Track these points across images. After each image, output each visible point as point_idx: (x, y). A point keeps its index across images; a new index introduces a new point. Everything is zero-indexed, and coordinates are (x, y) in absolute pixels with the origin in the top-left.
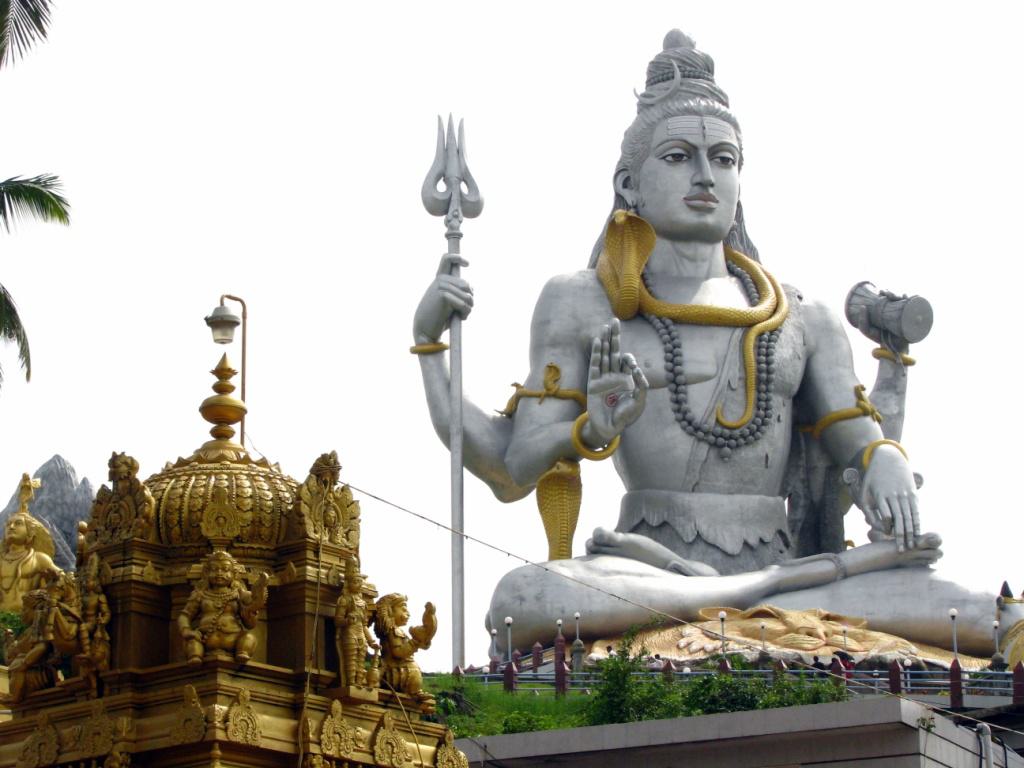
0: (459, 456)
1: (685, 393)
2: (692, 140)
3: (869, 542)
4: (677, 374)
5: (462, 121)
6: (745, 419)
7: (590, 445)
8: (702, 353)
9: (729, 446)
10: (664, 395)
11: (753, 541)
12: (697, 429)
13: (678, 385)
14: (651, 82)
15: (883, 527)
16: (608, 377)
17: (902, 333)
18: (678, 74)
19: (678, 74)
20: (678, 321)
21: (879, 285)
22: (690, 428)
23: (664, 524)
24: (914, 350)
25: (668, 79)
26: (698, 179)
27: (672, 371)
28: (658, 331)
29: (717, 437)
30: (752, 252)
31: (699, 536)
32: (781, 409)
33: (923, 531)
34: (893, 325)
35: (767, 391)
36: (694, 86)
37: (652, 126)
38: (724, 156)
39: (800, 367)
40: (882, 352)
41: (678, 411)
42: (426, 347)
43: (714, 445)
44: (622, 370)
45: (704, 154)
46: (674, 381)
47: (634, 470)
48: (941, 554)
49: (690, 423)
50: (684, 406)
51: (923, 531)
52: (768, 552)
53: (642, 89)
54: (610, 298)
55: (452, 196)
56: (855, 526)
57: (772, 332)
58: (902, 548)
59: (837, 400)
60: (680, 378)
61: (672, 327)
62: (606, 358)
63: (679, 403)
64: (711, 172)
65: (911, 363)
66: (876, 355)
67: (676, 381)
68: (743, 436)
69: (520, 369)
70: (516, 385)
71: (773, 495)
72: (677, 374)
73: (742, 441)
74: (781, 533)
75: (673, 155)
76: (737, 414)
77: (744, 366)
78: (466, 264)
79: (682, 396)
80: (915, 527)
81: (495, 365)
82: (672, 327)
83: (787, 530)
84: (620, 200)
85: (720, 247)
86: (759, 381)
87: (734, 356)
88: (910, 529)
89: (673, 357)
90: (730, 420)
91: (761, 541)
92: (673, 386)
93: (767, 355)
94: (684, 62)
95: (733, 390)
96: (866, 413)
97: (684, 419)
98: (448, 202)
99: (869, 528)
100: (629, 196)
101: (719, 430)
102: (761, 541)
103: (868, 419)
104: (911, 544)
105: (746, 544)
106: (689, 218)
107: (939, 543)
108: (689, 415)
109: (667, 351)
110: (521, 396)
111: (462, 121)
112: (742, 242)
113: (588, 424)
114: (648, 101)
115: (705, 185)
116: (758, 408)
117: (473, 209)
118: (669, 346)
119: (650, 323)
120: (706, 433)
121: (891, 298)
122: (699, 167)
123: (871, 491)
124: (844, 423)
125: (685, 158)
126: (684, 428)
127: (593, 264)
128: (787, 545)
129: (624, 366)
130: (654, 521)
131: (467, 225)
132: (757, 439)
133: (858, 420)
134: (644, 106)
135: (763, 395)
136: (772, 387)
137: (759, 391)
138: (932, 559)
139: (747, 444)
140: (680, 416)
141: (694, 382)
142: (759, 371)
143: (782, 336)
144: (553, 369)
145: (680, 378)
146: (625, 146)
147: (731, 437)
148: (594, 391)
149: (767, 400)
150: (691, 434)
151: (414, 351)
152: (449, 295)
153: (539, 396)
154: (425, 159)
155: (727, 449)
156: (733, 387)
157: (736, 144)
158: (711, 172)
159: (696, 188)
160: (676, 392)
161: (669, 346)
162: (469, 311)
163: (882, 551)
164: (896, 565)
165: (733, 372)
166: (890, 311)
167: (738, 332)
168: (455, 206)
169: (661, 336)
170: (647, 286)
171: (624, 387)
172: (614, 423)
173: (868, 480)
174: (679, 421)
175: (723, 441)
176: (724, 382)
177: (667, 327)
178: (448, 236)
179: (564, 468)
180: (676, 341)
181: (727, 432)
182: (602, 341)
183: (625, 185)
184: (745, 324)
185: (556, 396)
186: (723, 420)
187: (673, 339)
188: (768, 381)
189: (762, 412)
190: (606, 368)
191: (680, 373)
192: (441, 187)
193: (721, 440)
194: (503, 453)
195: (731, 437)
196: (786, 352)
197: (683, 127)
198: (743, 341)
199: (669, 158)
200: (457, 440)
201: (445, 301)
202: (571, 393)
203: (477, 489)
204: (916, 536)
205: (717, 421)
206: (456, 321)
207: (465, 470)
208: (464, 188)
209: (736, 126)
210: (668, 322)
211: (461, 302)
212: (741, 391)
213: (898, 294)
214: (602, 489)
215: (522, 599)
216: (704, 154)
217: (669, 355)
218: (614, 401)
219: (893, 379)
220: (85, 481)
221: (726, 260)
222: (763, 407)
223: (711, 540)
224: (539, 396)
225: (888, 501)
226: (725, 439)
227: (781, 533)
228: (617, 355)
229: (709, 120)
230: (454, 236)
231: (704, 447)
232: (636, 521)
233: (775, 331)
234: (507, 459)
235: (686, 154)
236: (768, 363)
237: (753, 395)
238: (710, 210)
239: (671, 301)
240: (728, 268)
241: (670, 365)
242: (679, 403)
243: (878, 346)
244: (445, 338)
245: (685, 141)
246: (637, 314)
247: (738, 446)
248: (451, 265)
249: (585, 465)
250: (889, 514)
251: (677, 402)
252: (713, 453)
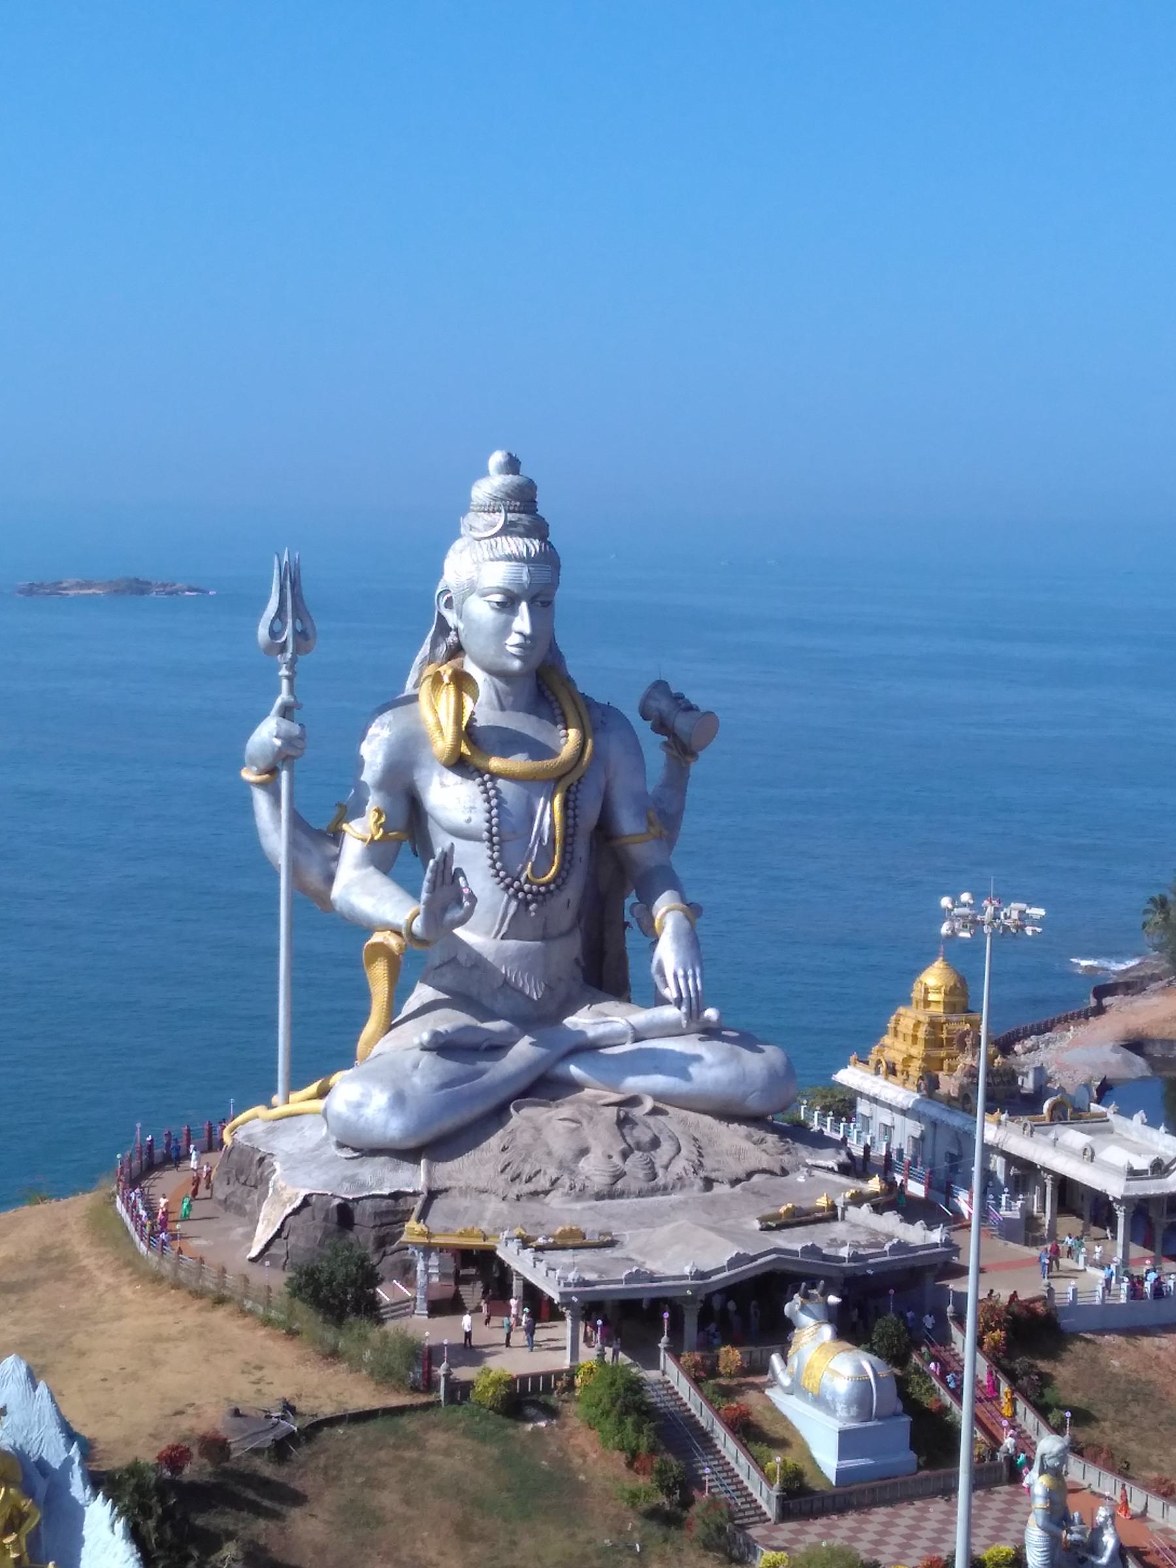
25: (494, 512)
29: (526, 893)
32: (582, 849)
59: (628, 822)
88: (694, 1007)
101: (526, 887)
135: (569, 849)
166: (682, 723)
190: (439, 880)
215: (361, 1116)
218: (445, 910)
219: (677, 777)
225: (676, 976)
243: (665, 738)
250: (675, 995)
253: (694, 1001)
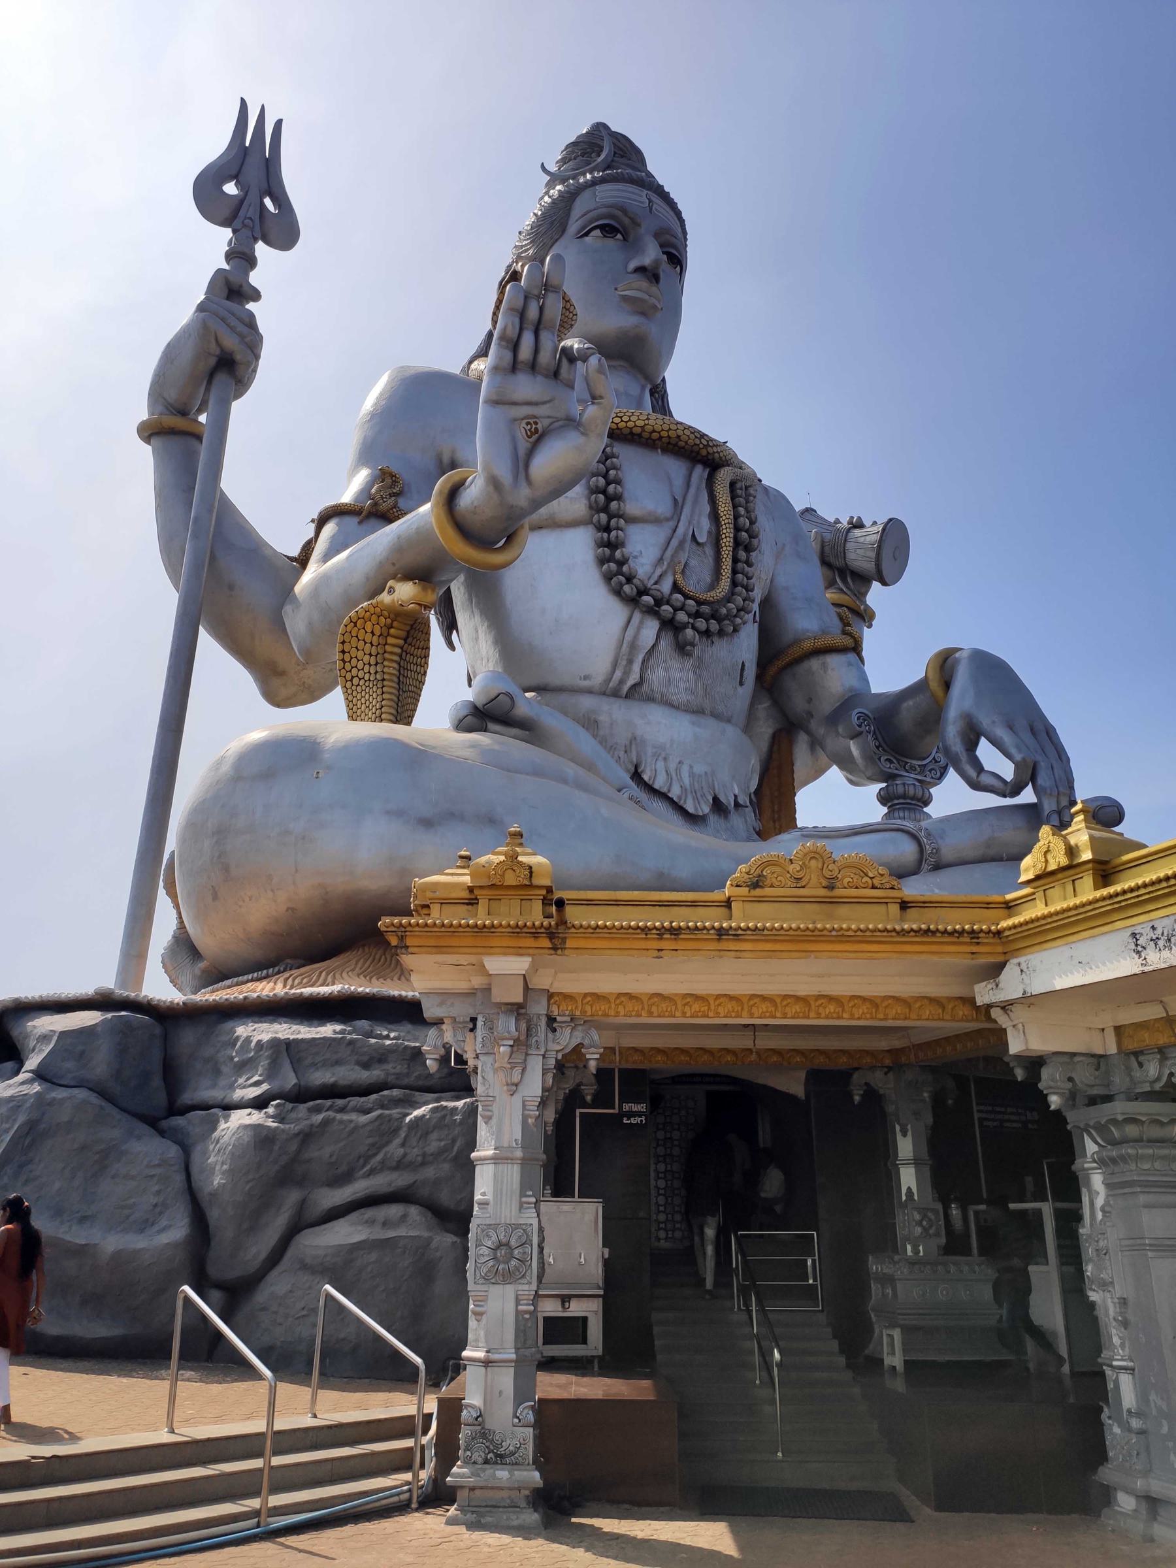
5: (279, 124)
9: (694, 628)
12: (643, 592)
13: (611, 517)
29: (676, 610)
43: (669, 625)
86: (737, 543)
91: (737, 805)
92: (603, 517)
95: (698, 544)
111: (279, 124)
116: (734, 584)
120: (659, 602)
125: (619, 236)
139: (721, 633)
142: (737, 529)
155: (689, 632)
156: (700, 541)
188: (748, 549)
199: (597, 232)
205: (676, 588)
212: (709, 551)
226: (689, 615)
248: (232, 290)
252: (666, 640)
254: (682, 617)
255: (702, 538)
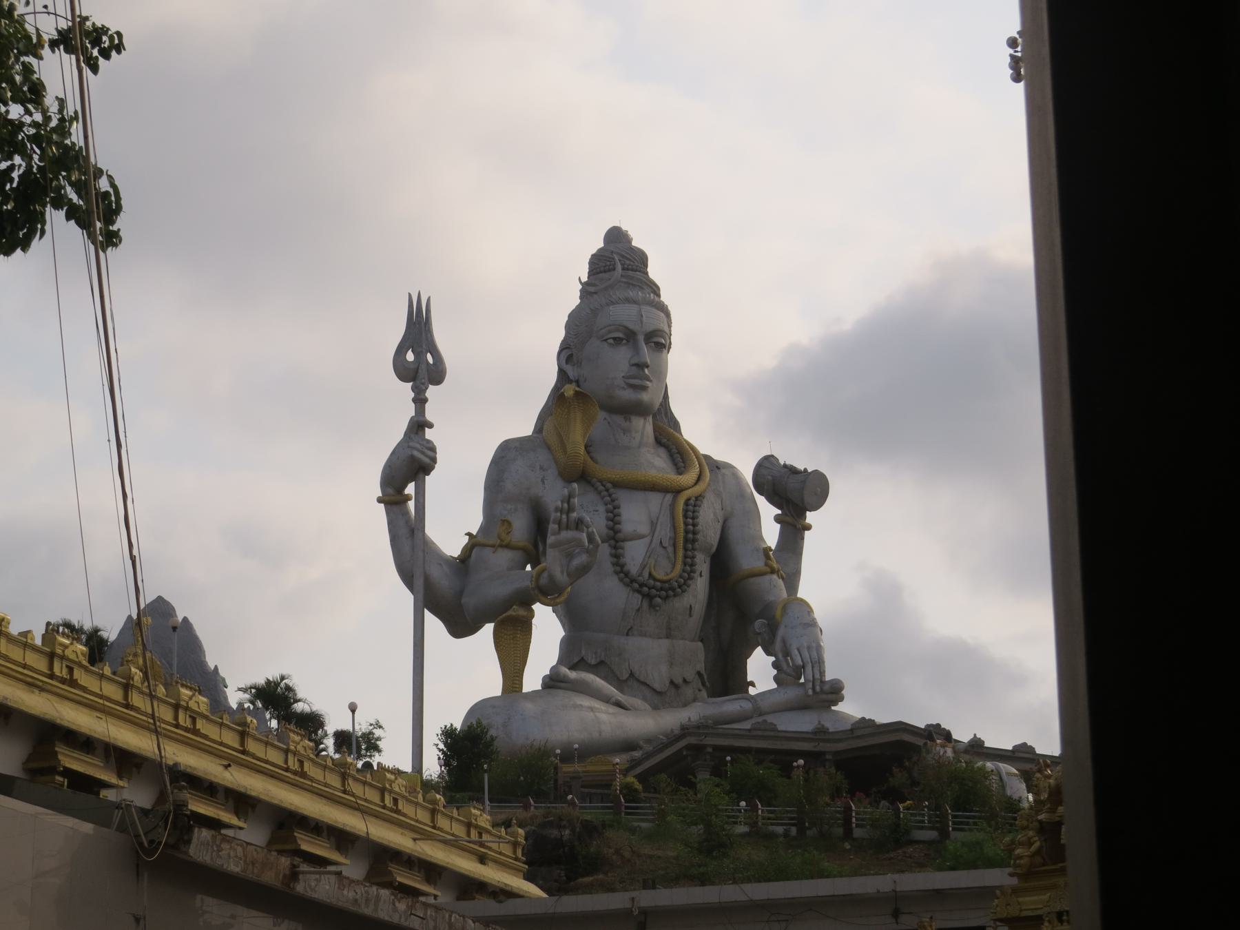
0: (421, 595)
1: (622, 548)
2: (631, 327)
3: (775, 686)
4: (616, 532)
6: (673, 575)
7: (547, 593)
8: (636, 514)
10: (605, 550)
11: (679, 681)
12: (633, 581)
14: (592, 273)
15: (785, 673)
16: (566, 535)
17: (802, 499)
18: (619, 267)
19: (619, 267)
20: (618, 485)
21: (783, 459)
22: (627, 580)
23: (602, 663)
24: (811, 517)
25: (609, 270)
26: (635, 361)
27: (612, 529)
28: (600, 493)
30: (675, 425)
31: (632, 675)
32: (703, 565)
33: (829, 677)
34: (796, 493)
35: (694, 549)
36: (632, 278)
37: (595, 312)
38: (659, 341)
39: (719, 527)
40: (788, 519)
41: (614, 564)
42: (393, 498)
44: (577, 528)
45: (641, 338)
46: (613, 538)
47: (572, 618)
48: (842, 699)
49: (627, 575)
50: (622, 560)
51: (829, 677)
52: (688, 692)
53: (585, 279)
54: (556, 462)
55: (419, 361)
56: (760, 670)
57: (697, 498)
58: (810, 692)
59: (747, 561)
60: (620, 535)
61: (612, 490)
62: (564, 516)
63: (617, 557)
64: (646, 354)
65: (809, 528)
66: (778, 519)
67: (615, 538)
68: (673, 590)
69: (474, 520)
70: (469, 534)
71: (693, 640)
72: (616, 532)
73: (671, 593)
74: (699, 673)
75: (614, 339)
76: (664, 571)
77: (674, 527)
78: (431, 426)
79: (620, 551)
80: (822, 673)
81: (454, 514)
82: (612, 490)
83: (703, 672)
84: (563, 376)
85: (650, 419)
86: (686, 540)
87: (665, 520)
88: (817, 676)
89: (614, 518)
90: (660, 575)
91: (685, 681)
92: (612, 542)
93: (693, 518)
94: (623, 256)
96: (773, 571)
97: (622, 571)
98: (417, 371)
99: (775, 672)
100: (570, 370)
102: (685, 681)
103: (775, 576)
104: (818, 688)
105: (672, 682)
106: (627, 395)
107: (841, 689)
108: (626, 568)
109: (607, 511)
110: (474, 544)
112: (666, 414)
113: (545, 575)
114: (592, 289)
115: (641, 366)
116: (685, 564)
117: (437, 375)
118: (610, 507)
119: (589, 482)
120: (642, 585)
121: (792, 470)
122: (637, 350)
123: (784, 641)
124: (752, 580)
126: (621, 580)
127: (539, 428)
128: (703, 684)
129: (579, 524)
130: (593, 662)
131: (432, 392)
132: (683, 591)
133: (767, 577)
134: (587, 291)
136: (697, 545)
137: (686, 549)
138: (835, 704)
140: (618, 569)
141: (631, 540)
142: (686, 532)
143: (705, 501)
144: (506, 523)
145: (620, 535)
146: (568, 327)
147: (662, 589)
148: (553, 546)
149: (693, 557)
150: (627, 585)
151: (380, 500)
152: (416, 453)
153: (493, 546)
154: (397, 330)
155: (658, 600)
157: (666, 329)
158: (646, 354)
159: (634, 368)
160: (615, 548)
161: (610, 507)
162: (433, 468)
163: (791, 694)
164: (801, 706)
165: (664, 532)
167: (669, 497)
168: (423, 372)
169: (603, 498)
170: (588, 453)
171: (579, 543)
172: (569, 575)
173: (781, 632)
174: (617, 573)
175: (655, 593)
176: (656, 541)
177: (607, 490)
178: (414, 400)
179: (522, 612)
180: (616, 503)
181: (658, 584)
182: (562, 502)
183: (569, 359)
184: (677, 491)
185: (508, 546)
186: (654, 573)
187: (613, 501)
188: (694, 541)
189: (688, 568)
191: (620, 531)
192: (410, 356)
193: (654, 592)
194: (460, 593)
195: (662, 589)
196: (709, 517)
197: (623, 314)
198: (673, 506)
199: (611, 341)
200: (419, 582)
201: (412, 458)
202: (521, 544)
203: (433, 624)
204: (823, 682)
205: (650, 574)
206: (421, 475)
207: (426, 611)
208: (430, 358)
209: (668, 315)
210: (609, 485)
211: (427, 460)
212: (670, 549)
213: (801, 467)
214: (547, 630)
216: (641, 338)
217: (611, 515)
218: (570, 556)
220: (185, 619)
221: (655, 431)
222: (689, 564)
223: (642, 679)
224: (493, 546)
227: (699, 673)
228: (574, 515)
229: (646, 309)
230: (420, 401)
231: (636, 599)
232: (576, 660)
233: (699, 498)
234: (463, 601)
235: (628, 337)
236: (694, 525)
237: (680, 553)
238: (644, 388)
239: (611, 467)
240: (656, 439)
241: (611, 523)
242: (617, 557)
243: (779, 512)
244: (410, 489)
245: (626, 328)
246: (581, 476)
247: (667, 597)
248: (419, 425)
249: (538, 608)
251: (617, 556)
252: (645, 605)
253: (818, 683)
254: (654, 592)
255: (666, 544)
